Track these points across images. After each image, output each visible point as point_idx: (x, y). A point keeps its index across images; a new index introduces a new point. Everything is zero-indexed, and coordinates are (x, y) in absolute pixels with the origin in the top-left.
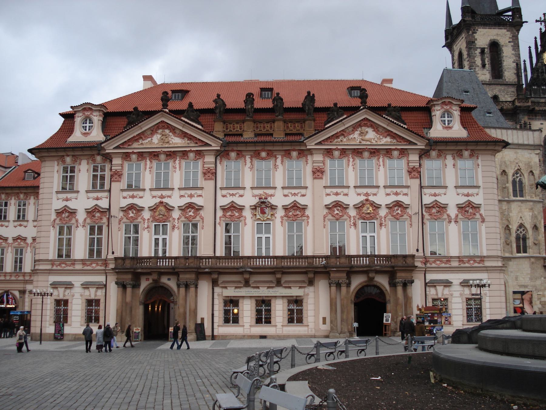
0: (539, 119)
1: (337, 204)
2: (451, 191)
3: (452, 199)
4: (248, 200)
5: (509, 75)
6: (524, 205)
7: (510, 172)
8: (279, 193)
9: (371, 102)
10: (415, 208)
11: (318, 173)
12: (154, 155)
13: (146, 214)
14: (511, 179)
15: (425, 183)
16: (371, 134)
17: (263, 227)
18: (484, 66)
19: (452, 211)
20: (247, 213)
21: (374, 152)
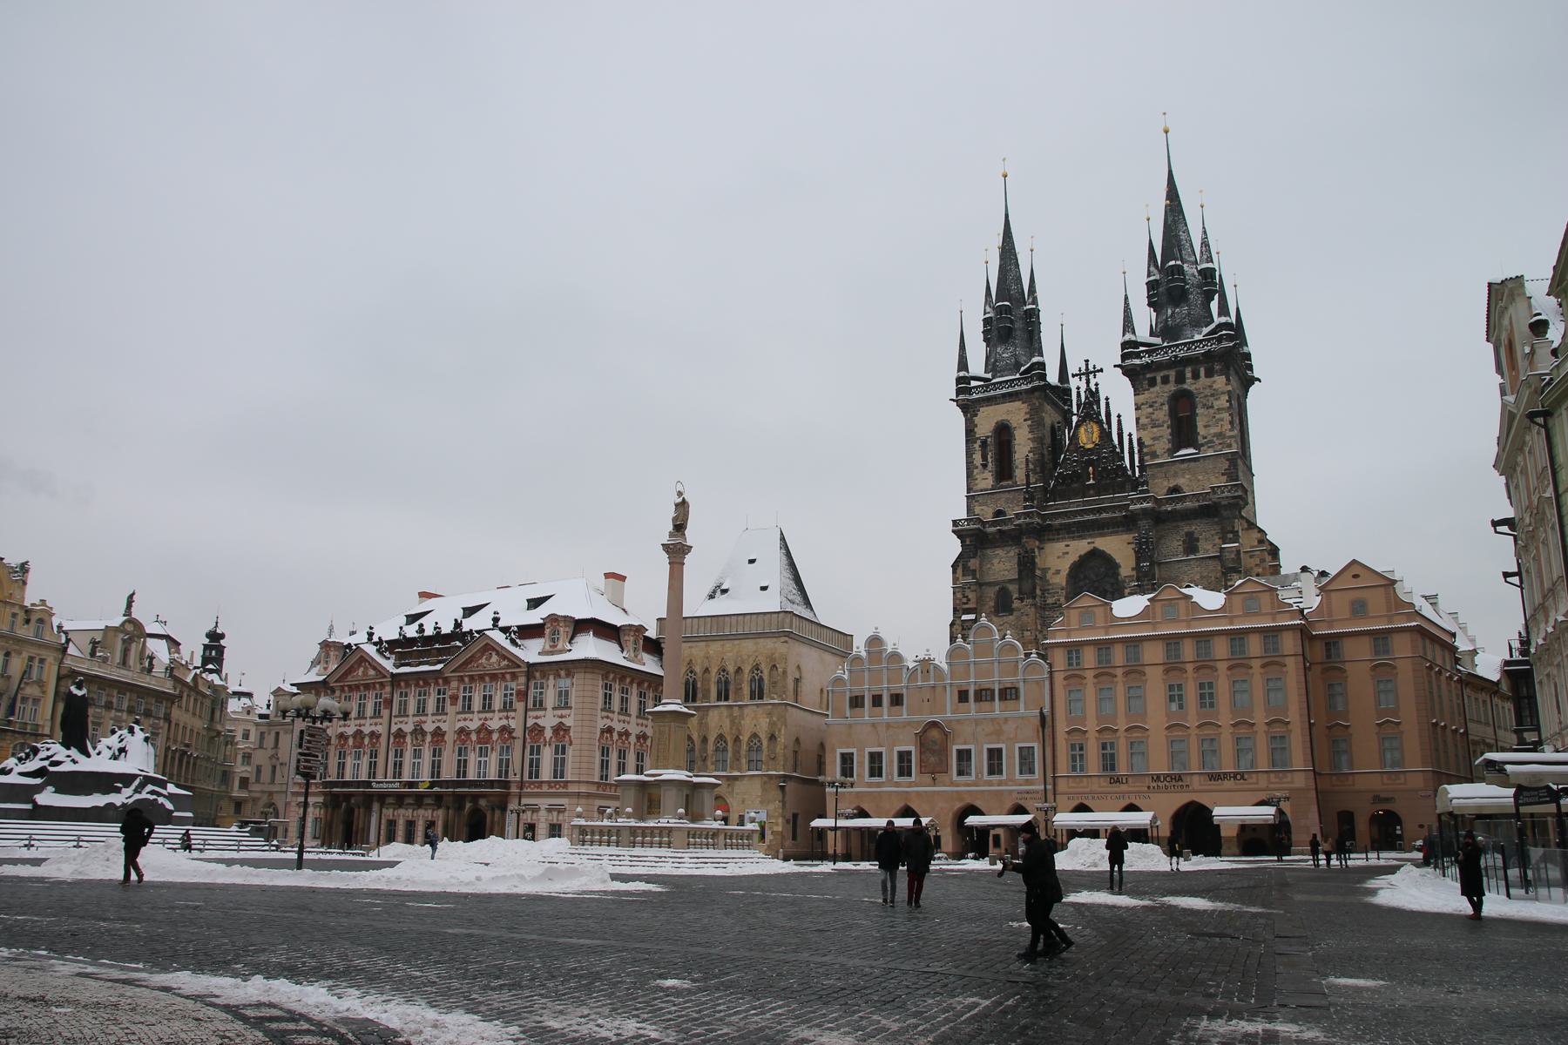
0: (1064, 539)
1: (462, 730)
2: (550, 712)
3: (548, 721)
4: (408, 728)
5: (1020, 474)
6: (760, 710)
7: (747, 669)
8: (430, 719)
9: (501, 624)
10: (518, 733)
11: (454, 699)
12: (357, 687)
13: (351, 741)
14: (746, 676)
15: (530, 705)
16: (495, 658)
17: (417, 754)
18: (985, 466)
19: (548, 734)
20: (408, 739)
21: (494, 677)
